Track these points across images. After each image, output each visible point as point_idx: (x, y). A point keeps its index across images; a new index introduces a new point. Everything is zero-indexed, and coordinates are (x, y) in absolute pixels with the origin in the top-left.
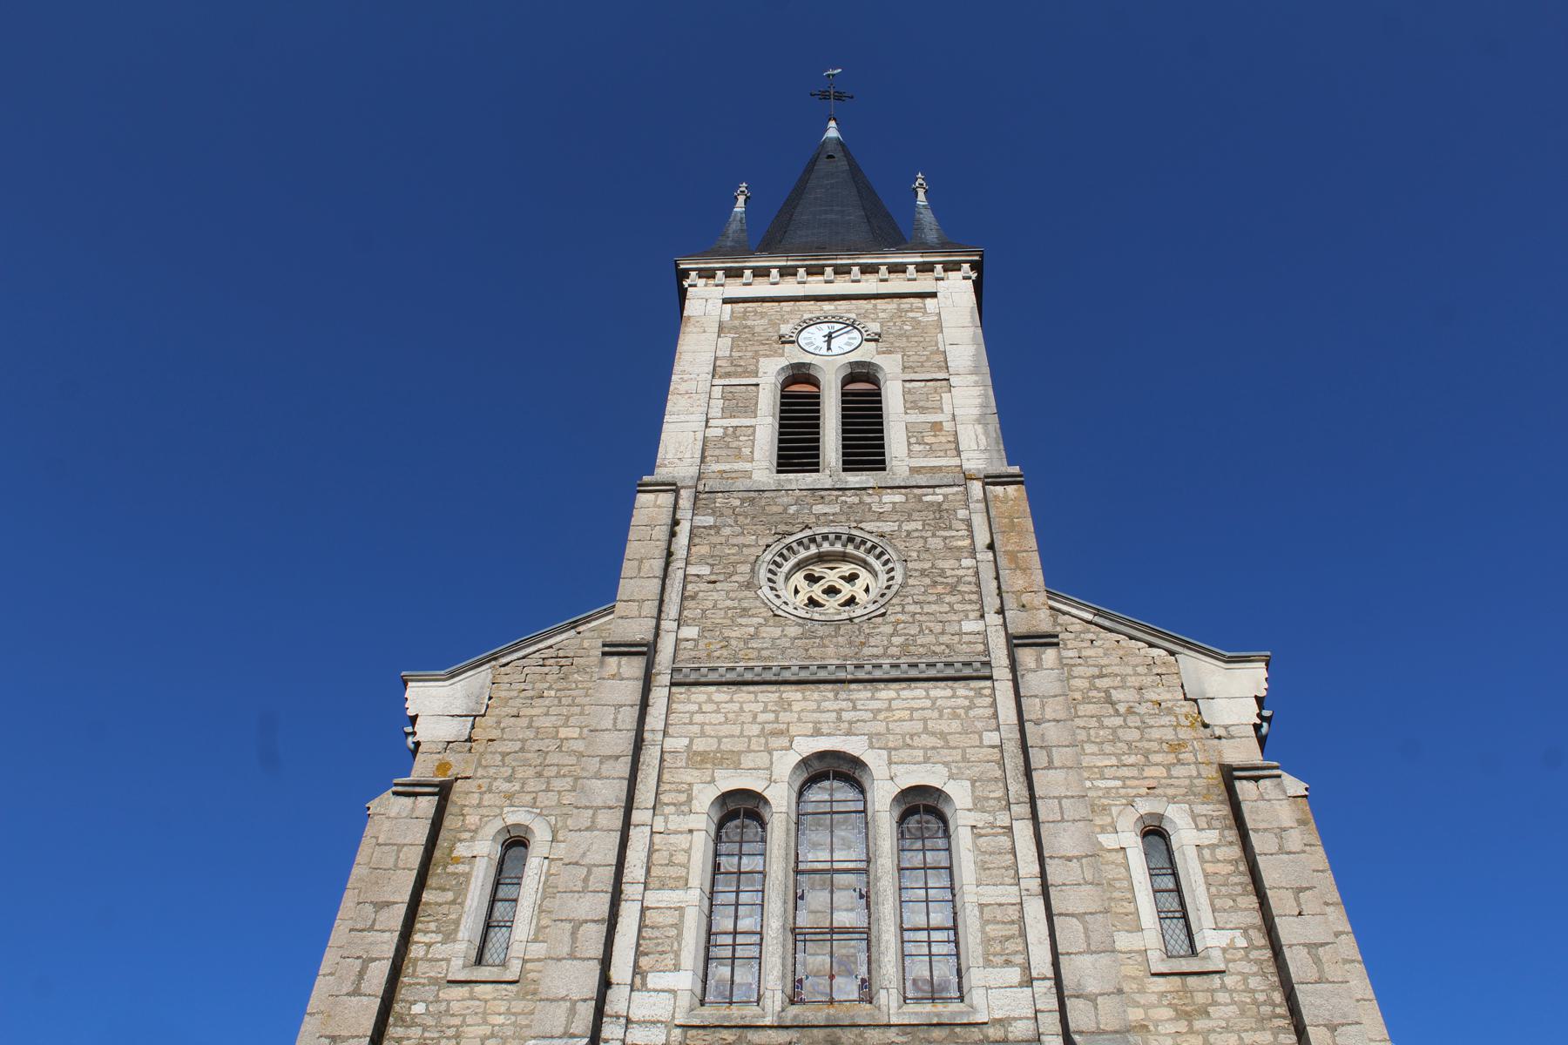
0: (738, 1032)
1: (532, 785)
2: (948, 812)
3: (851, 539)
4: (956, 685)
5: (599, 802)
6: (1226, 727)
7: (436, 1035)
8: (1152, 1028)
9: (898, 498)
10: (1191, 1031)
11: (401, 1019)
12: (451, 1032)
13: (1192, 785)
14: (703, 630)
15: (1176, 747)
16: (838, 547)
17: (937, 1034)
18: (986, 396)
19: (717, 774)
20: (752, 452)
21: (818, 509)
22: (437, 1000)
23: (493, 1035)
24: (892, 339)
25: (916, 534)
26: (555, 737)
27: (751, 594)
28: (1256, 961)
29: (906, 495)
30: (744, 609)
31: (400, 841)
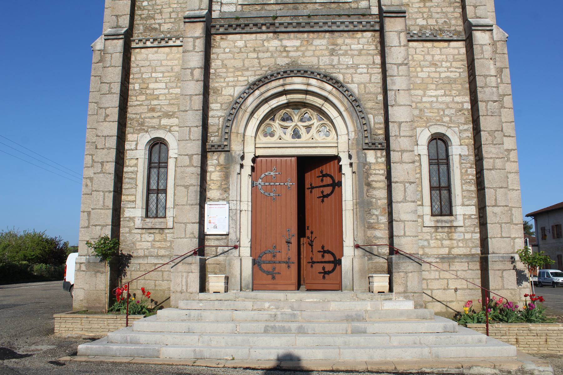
0: (262, 6)
7: (153, 13)
8: (410, 5)
10: (425, 6)
11: (139, 8)
17: (333, 6)
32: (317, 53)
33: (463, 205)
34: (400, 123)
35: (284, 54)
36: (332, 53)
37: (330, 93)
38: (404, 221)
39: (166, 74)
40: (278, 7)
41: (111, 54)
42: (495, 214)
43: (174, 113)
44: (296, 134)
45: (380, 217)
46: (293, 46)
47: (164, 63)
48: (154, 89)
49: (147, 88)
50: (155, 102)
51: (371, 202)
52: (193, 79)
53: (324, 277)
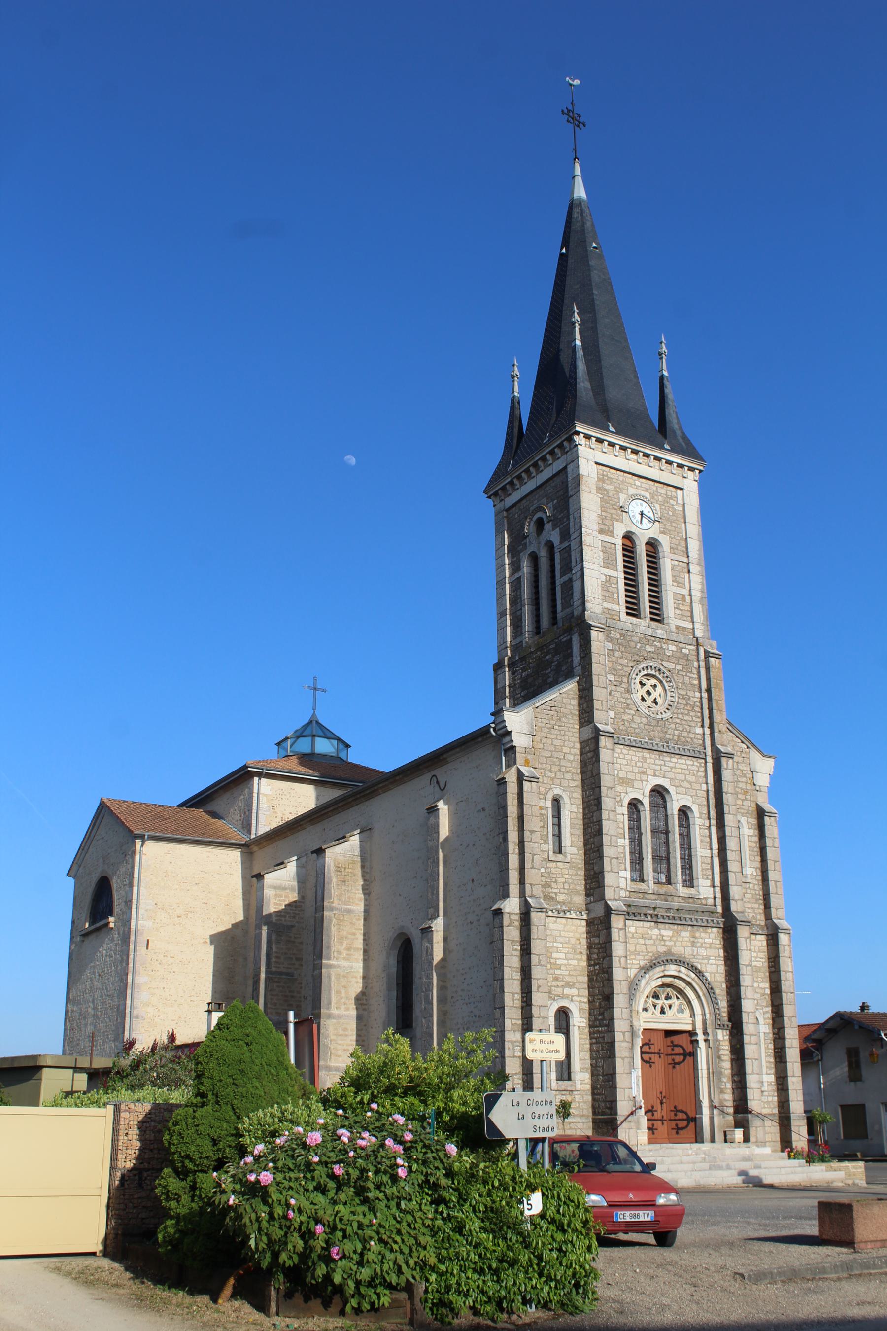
1: (559, 775)
2: (690, 815)
3: (659, 670)
4: (694, 759)
5: (609, 809)
6: (760, 786)
9: (673, 648)
12: (554, 880)
13: (748, 810)
14: (616, 714)
15: (746, 792)
16: (653, 672)
17: (691, 900)
18: (702, 583)
19: (629, 789)
20: (618, 597)
21: (648, 648)
22: (547, 867)
23: (566, 882)
24: (665, 522)
25: (680, 673)
26: (562, 752)
27: (627, 695)
28: (758, 880)
29: (676, 646)
30: (628, 705)
31: (531, 803)
32: (684, 944)
33: (767, 1074)
34: (748, 1013)
35: (662, 943)
36: (693, 944)
37: (693, 979)
38: (753, 1089)
39: (565, 945)
40: (654, 897)
41: (538, 926)
42: (793, 1082)
43: (574, 983)
44: (663, 1012)
45: (727, 1084)
46: (668, 936)
47: (563, 933)
48: (556, 959)
49: (551, 957)
50: (558, 972)
51: (721, 1072)
52: (621, 967)
53: (677, 1133)
